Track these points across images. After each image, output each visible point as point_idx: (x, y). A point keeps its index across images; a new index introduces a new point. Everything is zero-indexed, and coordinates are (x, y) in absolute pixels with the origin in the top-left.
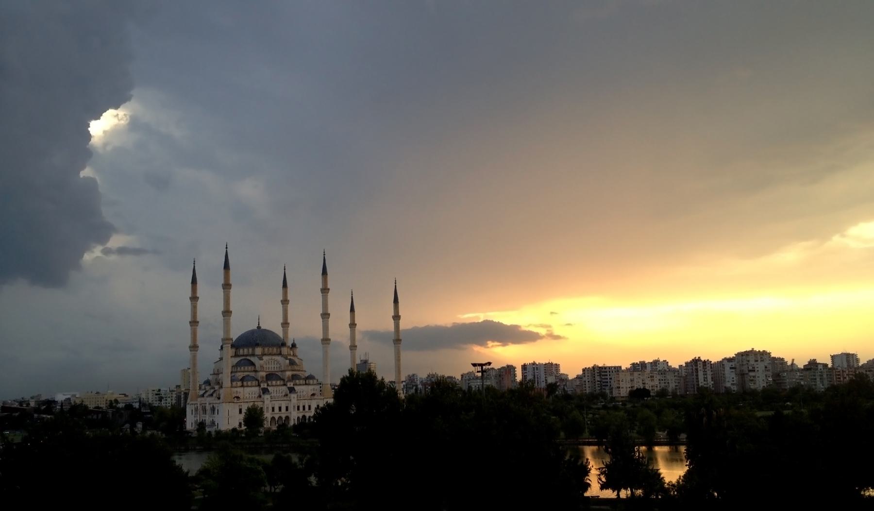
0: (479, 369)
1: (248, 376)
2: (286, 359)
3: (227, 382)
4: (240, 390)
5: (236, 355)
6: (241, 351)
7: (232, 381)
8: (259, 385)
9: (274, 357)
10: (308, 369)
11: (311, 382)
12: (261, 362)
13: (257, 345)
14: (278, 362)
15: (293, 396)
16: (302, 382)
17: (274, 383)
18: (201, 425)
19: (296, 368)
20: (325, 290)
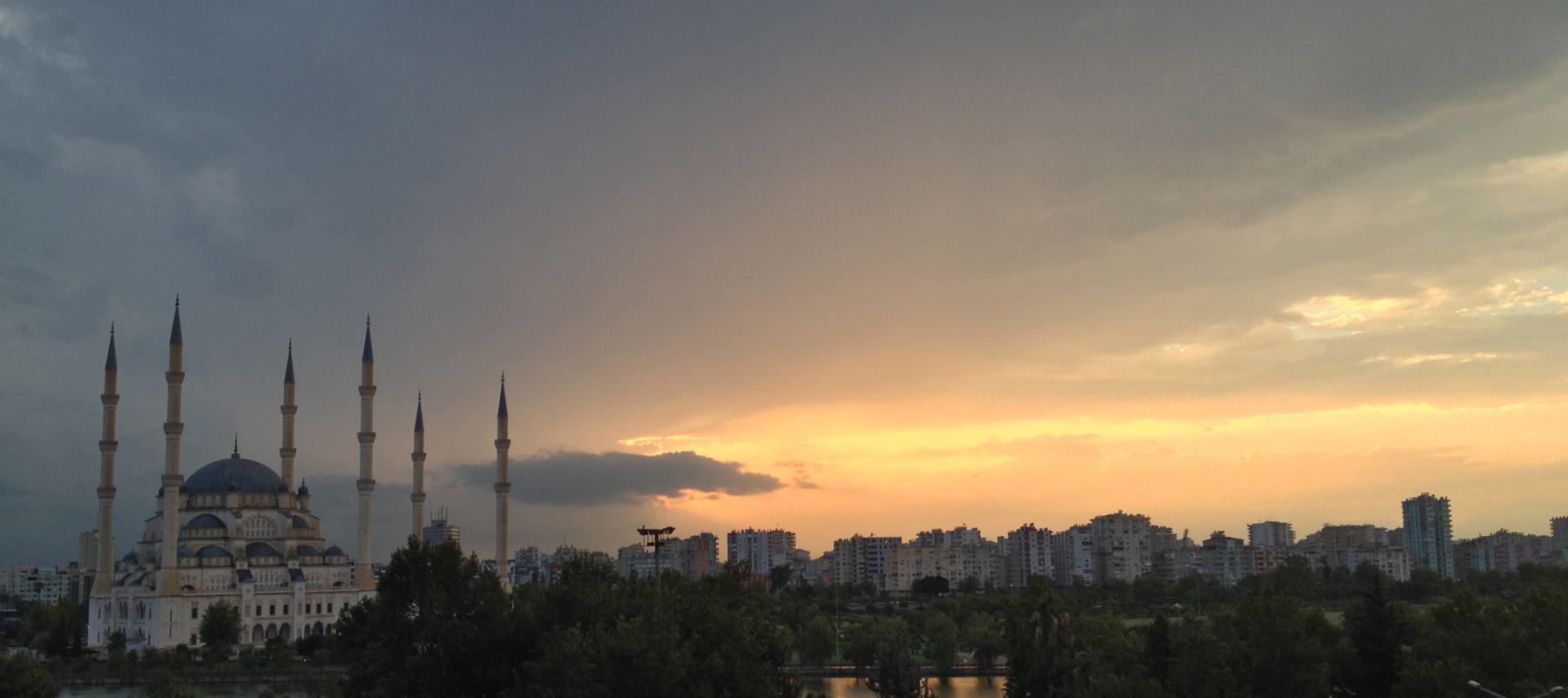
0: (651, 538)
1: (211, 547)
2: (288, 515)
3: (169, 557)
4: (196, 573)
5: (189, 508)
6: (200, 499)
7: (180, 556)
8: (233, 566)
9: (263, 513)
10: (331, 532)
11: (335, 559)
12: (239, 521)
13: (231, 489)
14: (271, 523)
15: (298, 585)
16: (316, 560)
17: (262, 561)
18: (117, 639)
19: (305, 533)
20: (367, 390)
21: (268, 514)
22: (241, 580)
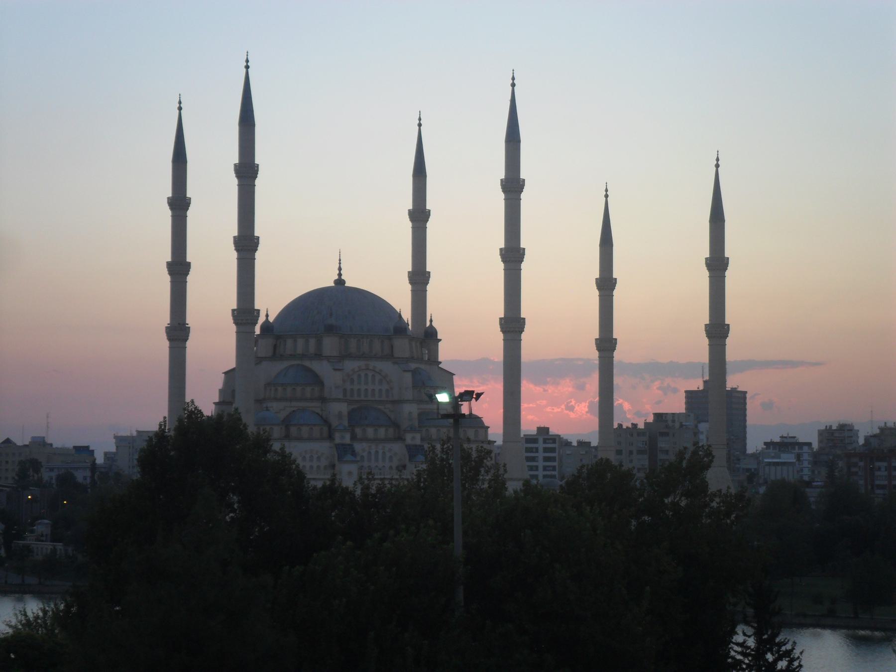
6: (289, 342)
8: (330, 437)
9: (372, 364)
17: (370, 432)
21: (380, 365)
22: (340, 458)
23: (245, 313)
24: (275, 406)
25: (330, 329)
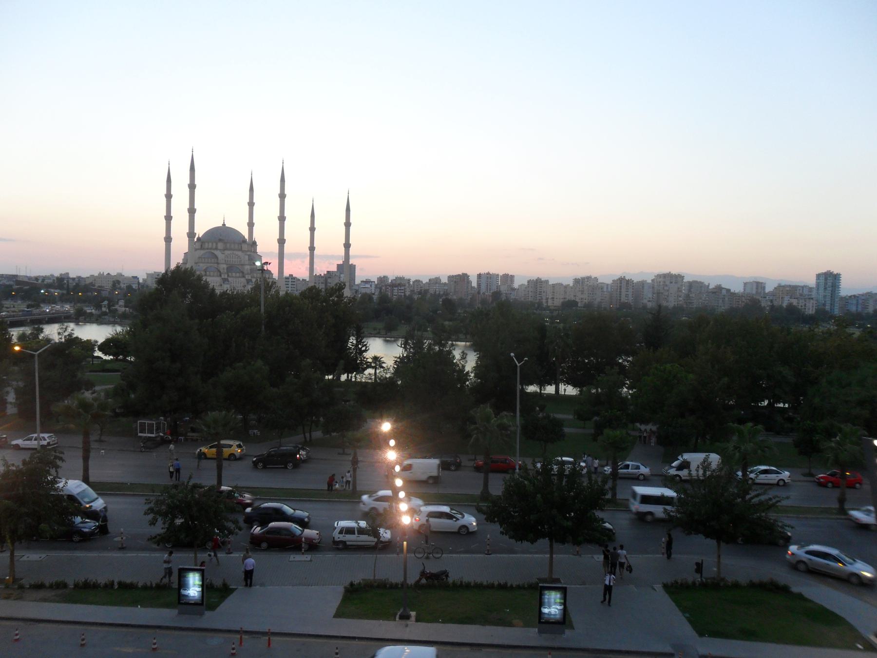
17: (234, 274)
23: (191, 234)
24: (201, 265)
25: (220, 240)
